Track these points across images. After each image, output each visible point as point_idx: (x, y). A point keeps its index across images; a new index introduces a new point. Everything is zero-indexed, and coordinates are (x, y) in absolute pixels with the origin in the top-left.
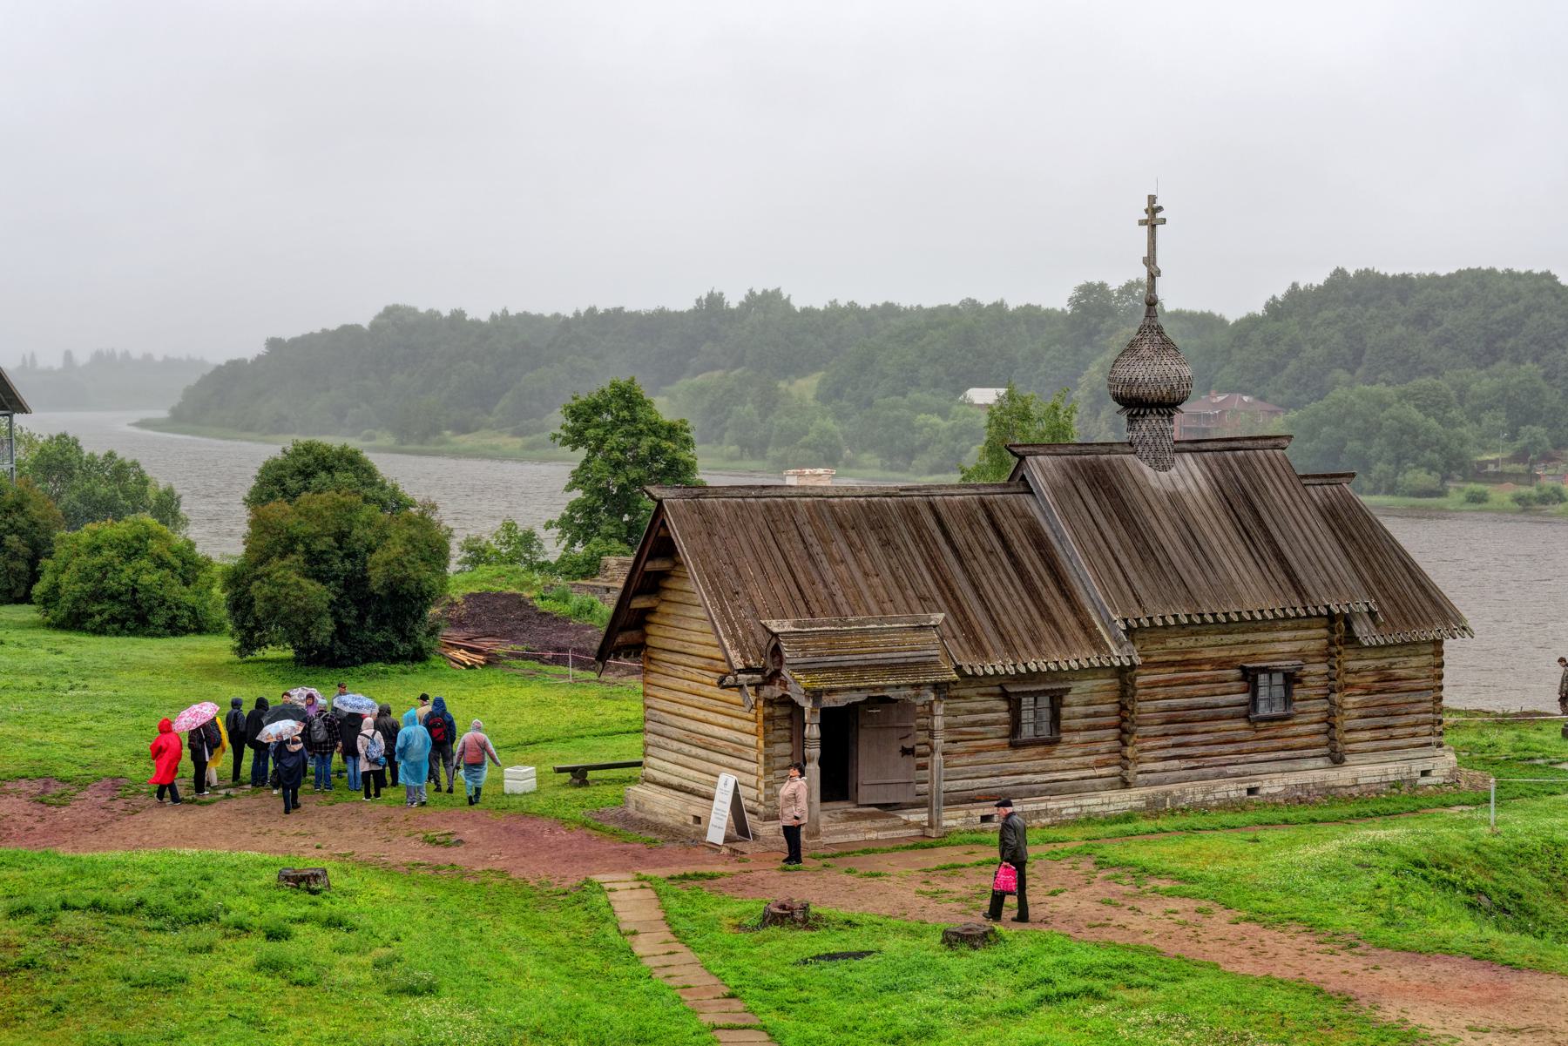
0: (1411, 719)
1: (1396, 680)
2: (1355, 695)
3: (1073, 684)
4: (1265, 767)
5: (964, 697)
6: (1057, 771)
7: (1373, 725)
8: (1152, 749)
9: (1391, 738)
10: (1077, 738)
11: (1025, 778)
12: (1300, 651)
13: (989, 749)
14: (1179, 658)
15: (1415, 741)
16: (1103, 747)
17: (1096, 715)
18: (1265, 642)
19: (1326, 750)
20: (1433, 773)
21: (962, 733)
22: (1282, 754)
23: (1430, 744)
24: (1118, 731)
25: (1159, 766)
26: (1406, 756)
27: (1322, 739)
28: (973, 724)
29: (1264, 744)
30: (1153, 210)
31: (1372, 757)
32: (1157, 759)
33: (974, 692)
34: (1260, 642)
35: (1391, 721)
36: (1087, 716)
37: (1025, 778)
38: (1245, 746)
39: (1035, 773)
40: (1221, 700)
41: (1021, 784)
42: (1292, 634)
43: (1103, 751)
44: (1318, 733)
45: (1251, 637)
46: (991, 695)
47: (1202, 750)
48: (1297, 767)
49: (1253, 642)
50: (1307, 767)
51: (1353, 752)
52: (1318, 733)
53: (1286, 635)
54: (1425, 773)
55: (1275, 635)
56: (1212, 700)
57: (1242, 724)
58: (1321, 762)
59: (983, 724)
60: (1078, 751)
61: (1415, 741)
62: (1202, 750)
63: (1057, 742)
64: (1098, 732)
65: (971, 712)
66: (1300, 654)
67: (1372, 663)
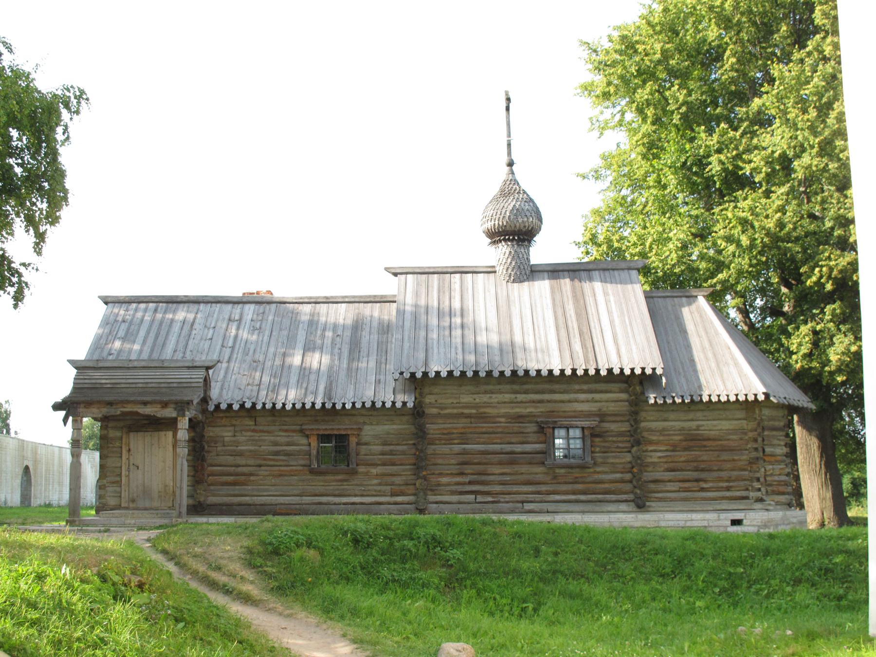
0: (723, 474)
1: (704, 440)
2: (660, 451)
3: (367, 428)
4: (564, 507)
5: (268, 432)
6: (356, 496)
7: (681, 477)
8: (449, 484)
9: (702, 490)
10: (374, 471)
11: (324, 499)
12: (600, 410)
13: (292, 474)
14: (474, 411)
15: (728, 494)
16: (397, 480)
17: (391, 453)
18: (563, 402)
19: (631, 497)
20: (745, 521)
21: (265, 459)
22: (583, 497)
23: (747, 498)
24: (415, 467)
25: (455, 498)
26: (718, 507)
27: (628, 487)
28: (277, 453)
29: (564, 487)
30: (508, 100)
31: (679, 505)
32: (453, 493)
33: (277, 428)
34: (555, 402)
35: (703, 475)
36: (383, 454)
37: (324, 499)
38: (544, 488)
39: (335, 496)
40: (519, 448)
41: (320, 503)
42: (589, 396)
43: (398, 482)
44: (622, 481)
45: (546, 397)
46: (294, 431)
47: (498, 488)
48: (597, 509)
49: (549, 401)
50: (609, 509)
51: (660, 500)
52: (622, 481)
53: (582, 396)
54: (736, 522)
55: (572, 396)
56: (508, 448)
57: (541, 469)
58: (623, 507)
59: (288, 454)
60: (375, 481)
61: (728, 494)
62: (498, 488)
63: (354, 472)
64: (395, 468)
65: (276, 444)
66: (602, 416)
67: (678, 424)
